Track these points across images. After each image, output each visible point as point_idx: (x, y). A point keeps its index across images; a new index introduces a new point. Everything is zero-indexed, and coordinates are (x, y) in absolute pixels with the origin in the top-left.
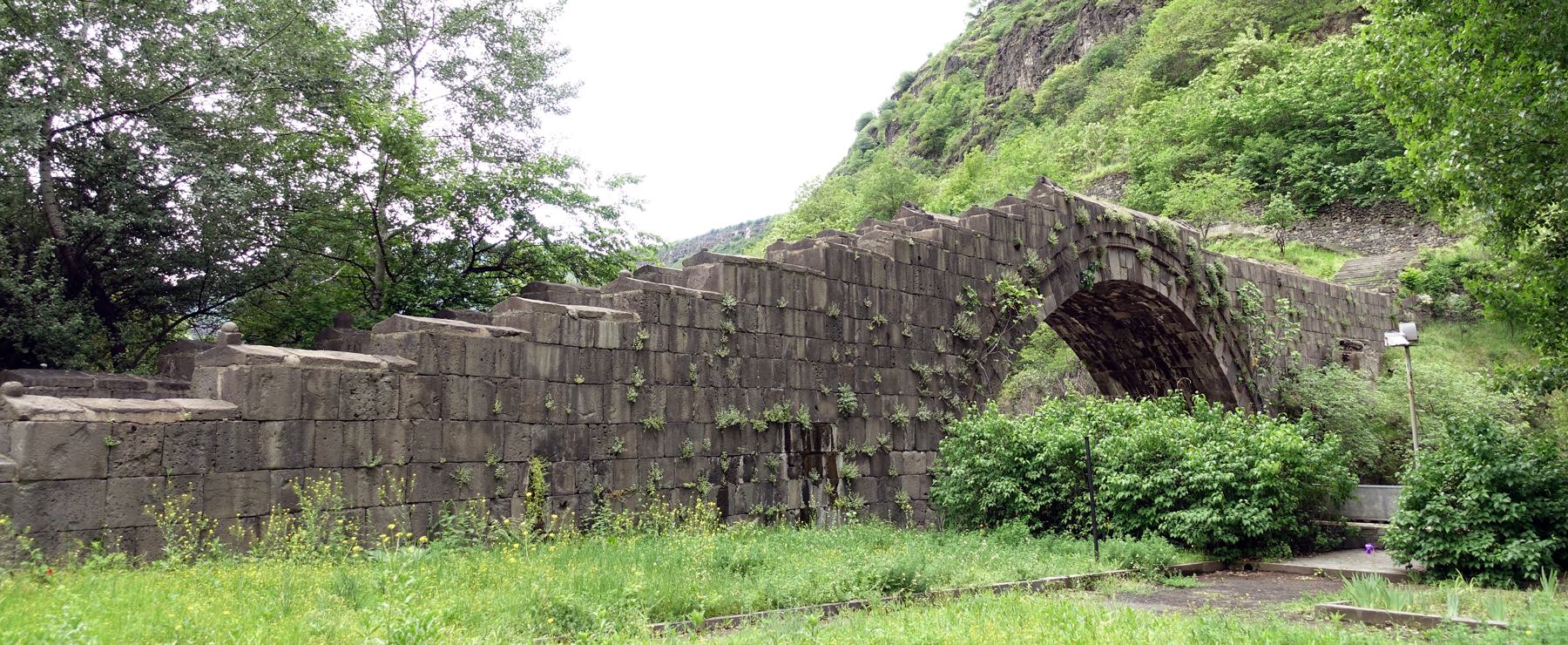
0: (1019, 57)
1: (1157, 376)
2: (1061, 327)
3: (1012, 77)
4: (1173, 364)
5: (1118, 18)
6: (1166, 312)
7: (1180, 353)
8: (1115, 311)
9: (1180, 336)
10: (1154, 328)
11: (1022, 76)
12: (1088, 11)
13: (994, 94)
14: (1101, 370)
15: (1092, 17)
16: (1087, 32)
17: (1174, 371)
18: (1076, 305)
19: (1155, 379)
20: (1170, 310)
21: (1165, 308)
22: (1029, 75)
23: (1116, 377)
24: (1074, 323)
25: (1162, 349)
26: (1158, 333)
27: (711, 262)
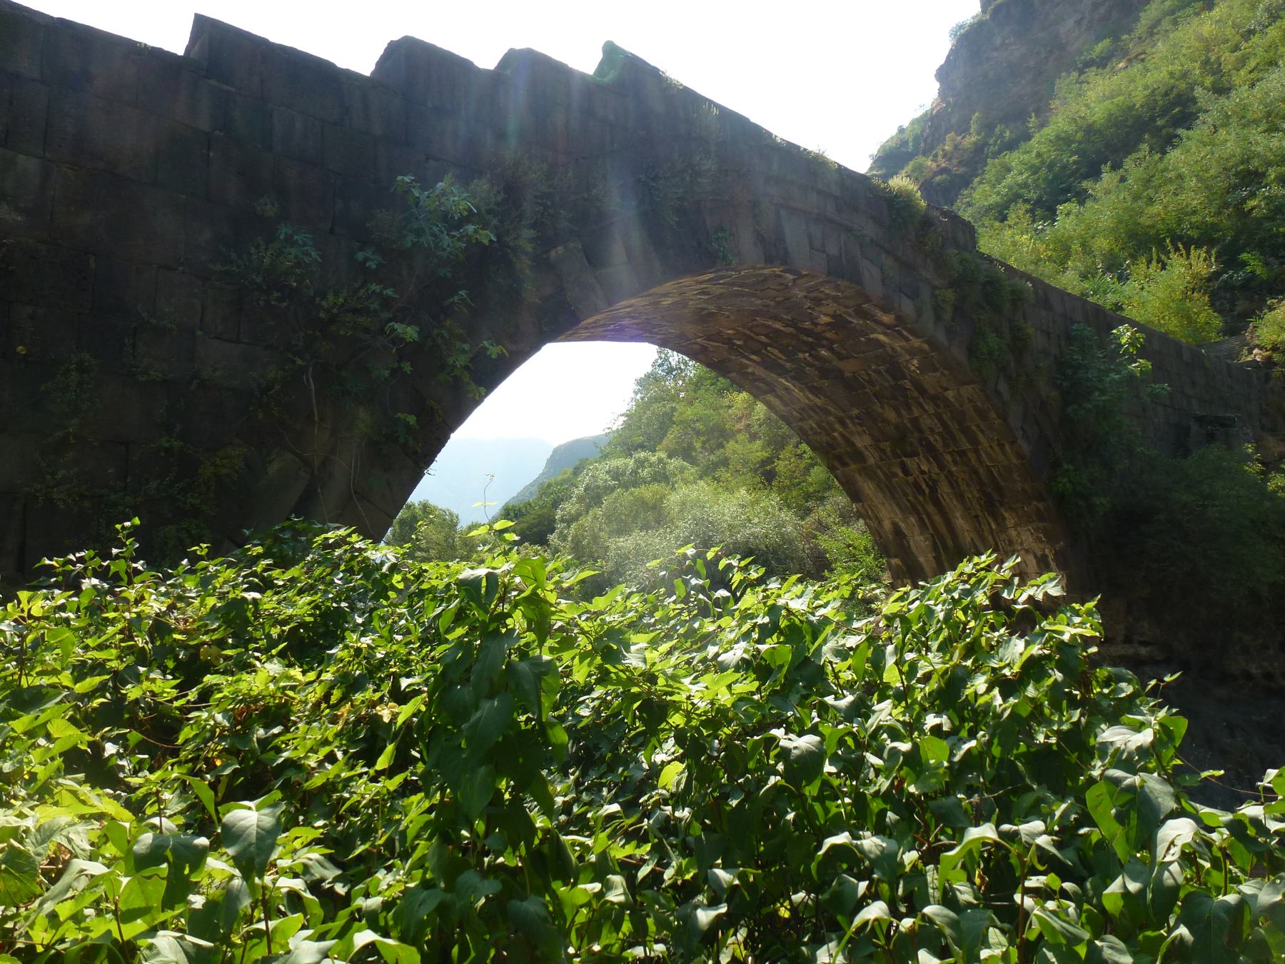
1: (925, 468)
2: (770, 398)
4: (946, 445)
6: (921, 351)
7: (954, 427)
8: (840, 357)
9: (950, 394)
10: (908, 385)
14: (845, 464)
17: (948, 458)
18: (776, 352)
19: (923, 472)
20: (926, 347)
21: (916, 342)
23: (869, 474)
24: (787, 389)
25: (926, 422)
26: (916, 394)
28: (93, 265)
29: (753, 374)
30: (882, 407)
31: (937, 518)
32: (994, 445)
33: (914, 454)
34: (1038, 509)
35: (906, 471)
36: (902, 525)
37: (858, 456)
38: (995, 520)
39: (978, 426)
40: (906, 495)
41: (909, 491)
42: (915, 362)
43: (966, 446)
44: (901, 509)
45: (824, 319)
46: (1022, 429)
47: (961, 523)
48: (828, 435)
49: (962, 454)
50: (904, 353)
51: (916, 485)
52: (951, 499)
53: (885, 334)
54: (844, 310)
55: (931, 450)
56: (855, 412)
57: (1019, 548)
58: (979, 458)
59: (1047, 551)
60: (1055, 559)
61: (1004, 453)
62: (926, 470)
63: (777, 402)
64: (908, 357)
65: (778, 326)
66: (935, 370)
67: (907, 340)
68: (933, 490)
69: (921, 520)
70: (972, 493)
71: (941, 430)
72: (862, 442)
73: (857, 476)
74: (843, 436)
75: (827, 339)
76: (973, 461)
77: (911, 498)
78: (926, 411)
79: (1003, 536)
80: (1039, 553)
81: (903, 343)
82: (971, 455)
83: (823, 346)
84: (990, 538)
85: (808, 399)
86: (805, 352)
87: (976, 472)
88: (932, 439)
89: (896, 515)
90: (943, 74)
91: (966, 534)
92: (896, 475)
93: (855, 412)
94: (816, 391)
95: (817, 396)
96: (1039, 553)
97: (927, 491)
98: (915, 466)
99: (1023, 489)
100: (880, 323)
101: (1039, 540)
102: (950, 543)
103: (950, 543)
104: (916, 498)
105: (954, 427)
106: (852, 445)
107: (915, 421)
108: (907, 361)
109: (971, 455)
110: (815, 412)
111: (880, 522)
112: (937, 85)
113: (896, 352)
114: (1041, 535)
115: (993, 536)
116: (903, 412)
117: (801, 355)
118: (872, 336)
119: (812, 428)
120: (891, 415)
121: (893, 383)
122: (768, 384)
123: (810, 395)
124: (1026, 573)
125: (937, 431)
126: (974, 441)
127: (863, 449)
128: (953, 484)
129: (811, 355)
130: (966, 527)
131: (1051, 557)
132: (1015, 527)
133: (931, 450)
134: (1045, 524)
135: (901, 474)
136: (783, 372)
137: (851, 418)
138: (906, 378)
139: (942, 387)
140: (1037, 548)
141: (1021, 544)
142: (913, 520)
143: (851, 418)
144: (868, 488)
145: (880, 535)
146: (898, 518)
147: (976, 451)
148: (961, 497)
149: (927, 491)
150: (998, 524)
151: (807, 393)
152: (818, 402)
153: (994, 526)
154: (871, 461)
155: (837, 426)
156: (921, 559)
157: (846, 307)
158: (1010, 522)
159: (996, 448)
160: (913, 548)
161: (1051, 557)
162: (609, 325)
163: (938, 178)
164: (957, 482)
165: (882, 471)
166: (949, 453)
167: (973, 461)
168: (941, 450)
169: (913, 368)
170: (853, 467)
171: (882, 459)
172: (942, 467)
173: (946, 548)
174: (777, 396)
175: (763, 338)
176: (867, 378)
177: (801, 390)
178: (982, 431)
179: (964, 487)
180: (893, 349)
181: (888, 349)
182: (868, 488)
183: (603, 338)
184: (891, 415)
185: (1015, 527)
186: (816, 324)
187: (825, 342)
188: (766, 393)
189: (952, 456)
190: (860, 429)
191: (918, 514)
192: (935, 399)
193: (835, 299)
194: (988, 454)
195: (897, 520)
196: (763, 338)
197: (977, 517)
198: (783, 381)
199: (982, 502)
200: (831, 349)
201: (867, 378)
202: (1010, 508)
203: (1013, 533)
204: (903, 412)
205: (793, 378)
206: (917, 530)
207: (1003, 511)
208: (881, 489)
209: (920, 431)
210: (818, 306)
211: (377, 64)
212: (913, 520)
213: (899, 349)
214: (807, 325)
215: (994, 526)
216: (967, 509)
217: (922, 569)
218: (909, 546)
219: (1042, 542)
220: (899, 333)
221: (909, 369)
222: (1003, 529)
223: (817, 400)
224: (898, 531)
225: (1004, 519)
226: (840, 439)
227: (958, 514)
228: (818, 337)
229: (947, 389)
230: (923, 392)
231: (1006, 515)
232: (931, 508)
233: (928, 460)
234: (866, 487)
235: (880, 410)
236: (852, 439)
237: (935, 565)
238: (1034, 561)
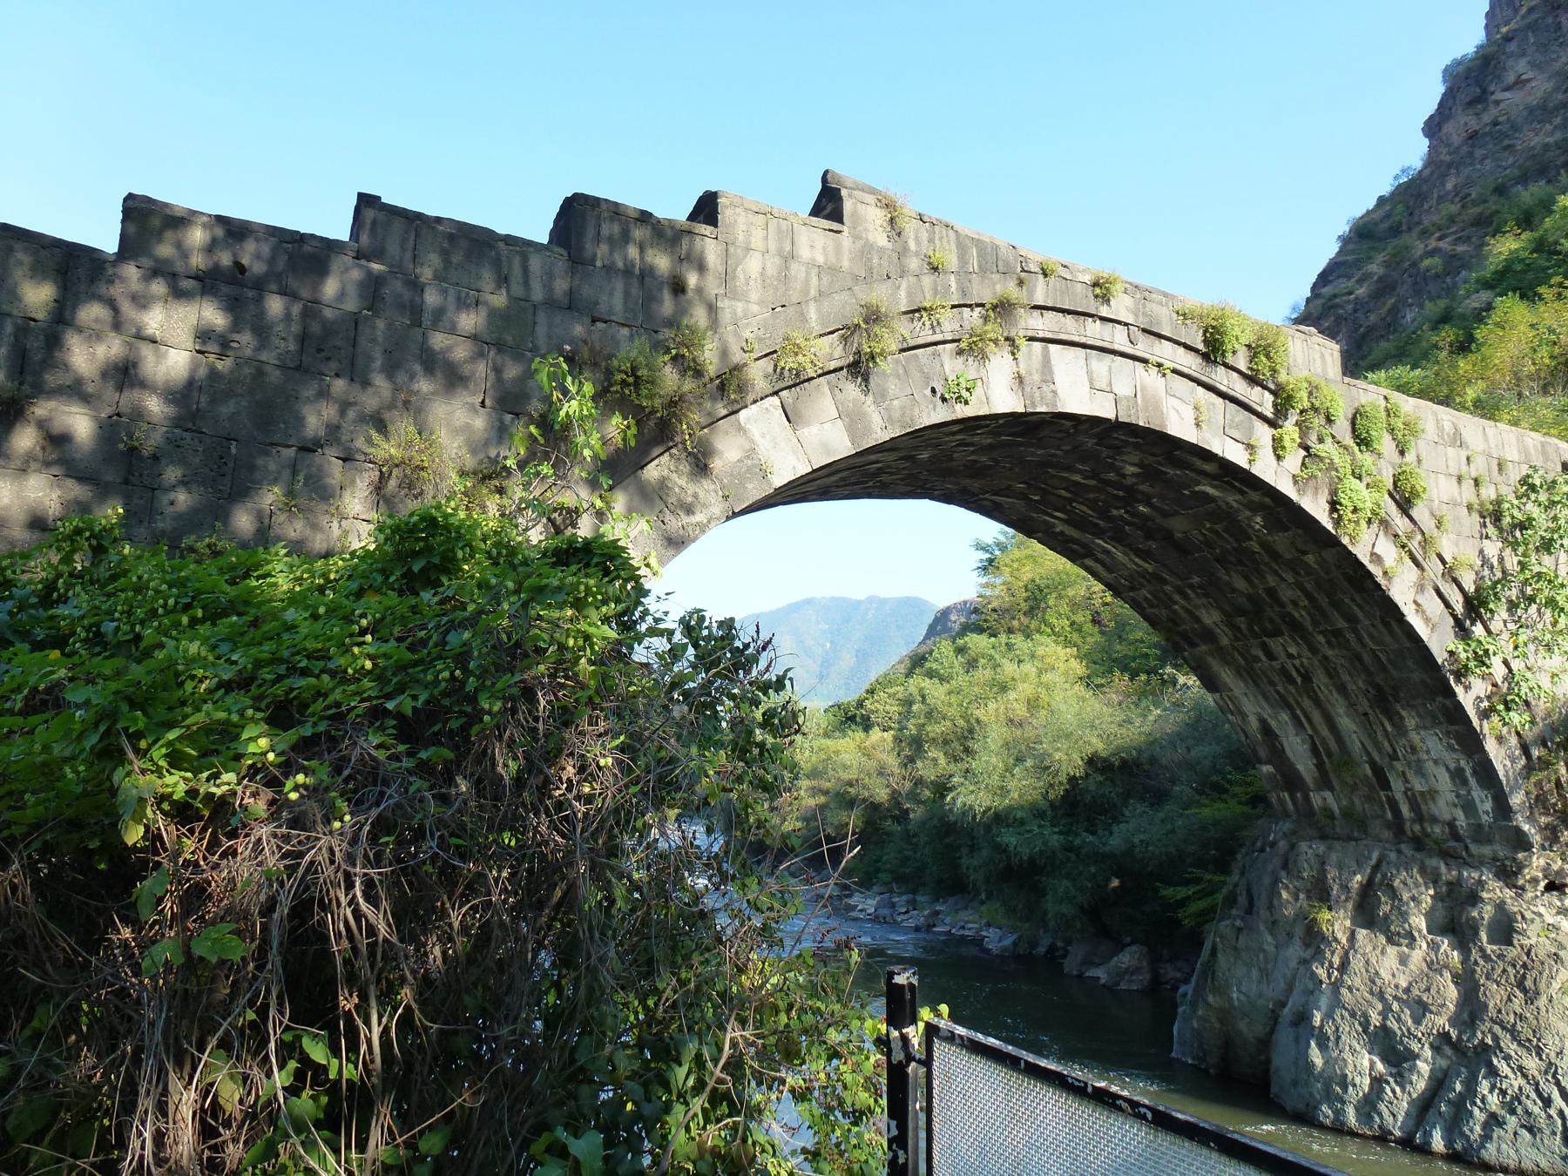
1: (1293, 650)
4: (1315, 623)
7: (1323, 600)
9: (1310, 559)
10: (1257, 548)
14: (1193, 645)
15: (1416, 283)
17: (1321, 639)
19: (1290, 656)
20: (1267, 500)
21: (1255, 496)
24: (1107, 552)
25: (1286, 594)
26: (1267, 560)
28: (234, 451)
29: (1062, 533)
30: (1227, 573)
31: (1317, 716)
32: (1377, 622)
33: (1277, 633)
34: (1444, 705)
35: (1271, 656)
36: (1272, 723)
37: (1209, 636)
38: (1390, 719)
39: (1353, 600)
40: (1272, 684)
41: (1276, 679)
42: (1259, 519)
43: (1341, 624)
44: (1268, 703)
45: (1131, 469)
46: (1415, 602)
47: (1346, 723)
48: (1168, 607)
49: (1338, 633)
50: (1241, 508)
51: (1284, 671)
52: (1330, 692)
53: (1213, 486)
54: (1151, 458)
55: (1295, 627)
56: (1196, 580)
57: (1425, 757)
58: (1360, 639)
59: (1463, 763)
60: (1475, 773)
61: (1391, 633)
62: (1295, 653)
63: (1099, 568)
64: (1248, 513)
65: (1077, 478)
66: (1287, 529)
67: (1242, 493)
68: (1307, 678)
69: (1295, 717)
70: (1356, 684)
71: (1306, 602)
72: (1210, 618)
73: (1210, 659)
74: (1183, 607)
75: (1142, 493)
76: (1354, 643)
77: (1280, 688)
78: (1284, 580)
79: (1403, 741)
80: (1452, 766)
81: (1238, 497)
82: (1350, 636)
83: (1140, 502)
84: (1386, 744)
85: (1136, 564)
86: (1118, 508)
87: (1358, 657)
88: (1297, 615)
89: (1263, 708)
90: (1433, 128)
91: (1354, 736)
92: (1257, 659)
93: (1196, 580)
94: (1145, 555)
95: (1144, 560)
96: (1452, 766)
97: (1299, 680)
98: (1280, 649)
99: (1423, 682)
100: (1203, 473)
101: (1450, 748)
102: (1333, 744)
103: (1333, 744)
104: (1285, 689)
105: (1323, 600)
106: (1198, 620)
107: (1271, 592)
108: (1249, 519)
109: (1350, 636)
110: (1144, 578)
111: (1244, 716)
112: (1426, 142)
113: (1232, 507)
114: (1453, 742)
115: (1389, 741)
116: (1256, 581)
117: (1115, 512)
118: (1197, 489)
119: (1146, 599)
120: (1241, 584)
121: (1235, 545)
122: (1084, 546)
123: (1137, 560)
124: (1437, 792)
125: (1301, 604)
126: (1351, 619)
127: (1213, 626)
128: (1332, 674)
129: (1126, 512)
130: (1353, 727)
131: (1468, 772)
132: (1418, 728)
133: (1295, 627)
134: (1456, 727)
135: (1264, 659)
136: (1099, 533)
137: (1191, 587)
138: (1251, 539)
139: (1298, 550)
140: (1451, 759)
141: (1428, 752)
142: (1287, 718)
143: (1191, 587)
144: (1226, 676)
145: (1244, 732)
146: (1267, 713)
147: (1355, 631)
148: (1342, 689)
149: (1299, 680)
150: (1393, 725)
151: (1133, 557)
152: (1149, 567)
153: (1389, 728)
154: (1225, 641)
155: (1177, 597)
156: (1300, 767)
157: (1153, 455)
158: (1411, 722)
159: (1381, 627)
160: (1287, 749)
161: (1468, 772)
162: (867, 482)
163: (1427, 262)
164: (1335, 669)
165: (1240, 654)
166: (1320, 632)
167: (1354, 643)
168: (1311, 629)
169: (1257, 527)
170: (1204, 648)
171: (1237, 639)
172: (1314, 651)
173: (1329, 754)
174: (1097, 560)
175: (1063, 493)
176: (1201, 538)
177: (1125, 554)
178: (1359, 606)
179: (1346, 678)
180: (1227, 504)
181: (1220, 503)
182: (1226, 676)
183: (870, 496)
184: (1241, 584)
185: (1418, 728)
186: (1124, 476)
187: (1140, 497)
188: (1085, 557)
189: (1325, 636)
190: (1204, 600)
191: (1289, 707)
192: (1293, 566)
193: (1136, 446)
194: (1371, 637)
195: (1266, 716)
196: (1063, 493)
197: (1366, 714)
198: (1101, 542)
199: (1371, 696)
200: (1149, 504)
201: (1201, 538)
202: (1408, 705)
203: (1415, 737)
204: (1256, 581)
205: (1112, 538)
206: (1291, 729)
207: (1398, 707)
208: (1241, 676)
209: (1282, 606)
210: (1121, 454)
211: (556, 221)
212: (1285, 716)
213: (1235, 505)
214: (1112, 476)
215: (1389, 728)
216: (1351, 705)
217: (1302, 780)
218: (1283, 750)
219: (1454, 750)
220: (1225, 482)
221: (1253, 528)
222: (1401, 730)
223: (1146, 565)
224: (1266, 729)
225: (1402, 718)
226: (1181, 612)
227: (1341, 711)
228: (1131, 490)
229: (1305, 553)
230: (1275, 555)
231: (1404, 713)
232: (1307, 703)
233: (1294, 640)
234: (1223, 673)
235: (1227, 578)
236: (1197, 613)
237: (1317, 774)
238: (1447, 775)
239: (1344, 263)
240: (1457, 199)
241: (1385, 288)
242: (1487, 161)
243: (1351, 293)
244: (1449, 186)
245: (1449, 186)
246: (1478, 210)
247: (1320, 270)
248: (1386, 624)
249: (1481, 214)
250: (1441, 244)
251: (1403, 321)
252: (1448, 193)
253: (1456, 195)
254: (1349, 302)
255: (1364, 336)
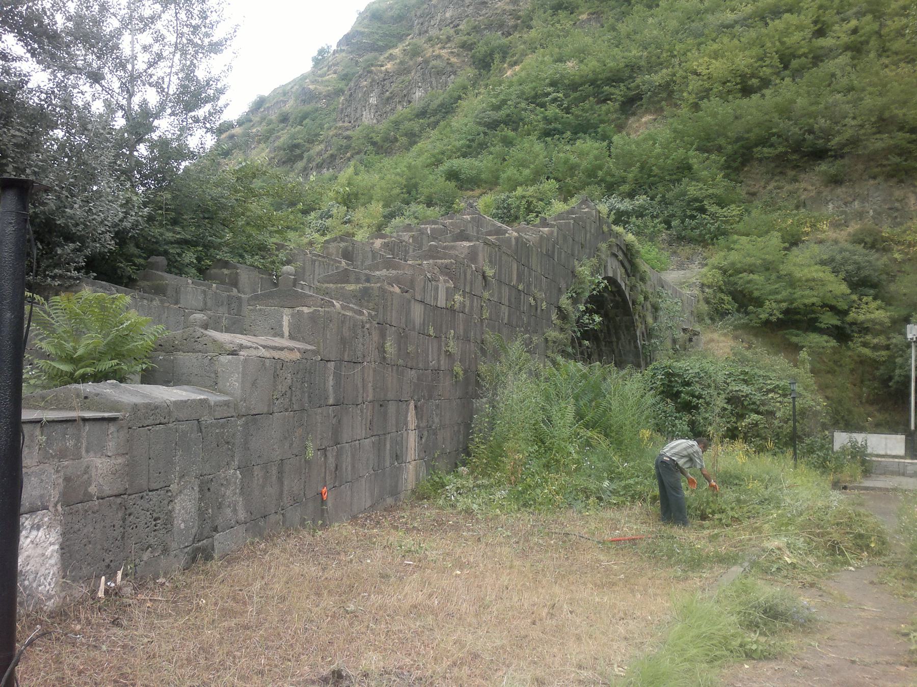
0: (367, 95)
3: (359, 111)
5: (443, 78)
7: (613, 331)
11: (367, 110)
12: (422, 68)
13: (344, 122)
15: (423, 74)
16: (420, 84)
22: (372, 111)
27: (470, 241)
43: (614, 339)
76: (615, 347)
82: (615, 344)
126: (618, 339)
239: (362, 33)
240: (451, 26)
241: (403, 70)
242: (471, 8)
243: (382, 66)
244: (448, 15)
245: (448, 15)
246: (465, 38)
247: (346, 33)
248: (630, 342)
249: (465, 42)
250: (443, 52)
251: (414, 96)
252: (446, 19)
253: (452, 23)
254: (381, 72)
255: (388, 99)
